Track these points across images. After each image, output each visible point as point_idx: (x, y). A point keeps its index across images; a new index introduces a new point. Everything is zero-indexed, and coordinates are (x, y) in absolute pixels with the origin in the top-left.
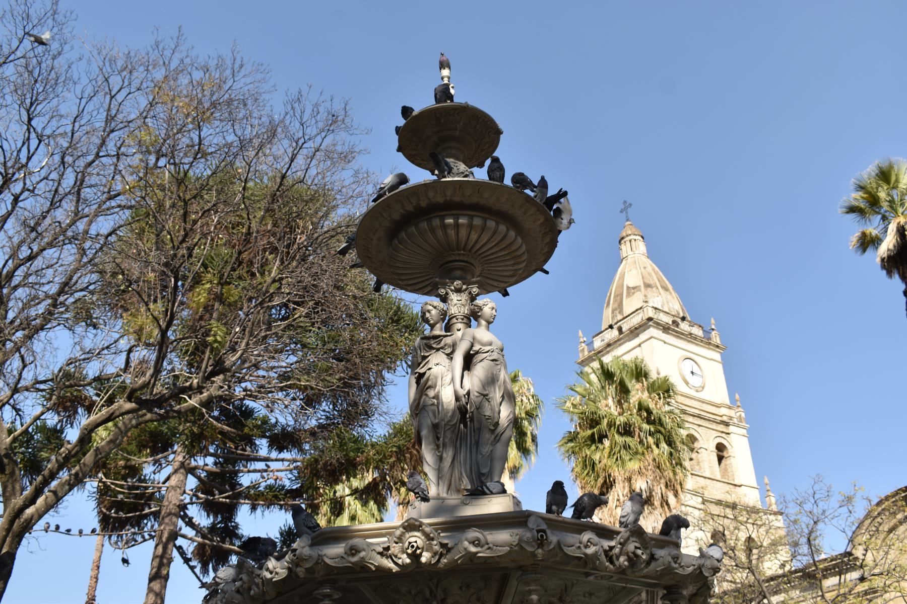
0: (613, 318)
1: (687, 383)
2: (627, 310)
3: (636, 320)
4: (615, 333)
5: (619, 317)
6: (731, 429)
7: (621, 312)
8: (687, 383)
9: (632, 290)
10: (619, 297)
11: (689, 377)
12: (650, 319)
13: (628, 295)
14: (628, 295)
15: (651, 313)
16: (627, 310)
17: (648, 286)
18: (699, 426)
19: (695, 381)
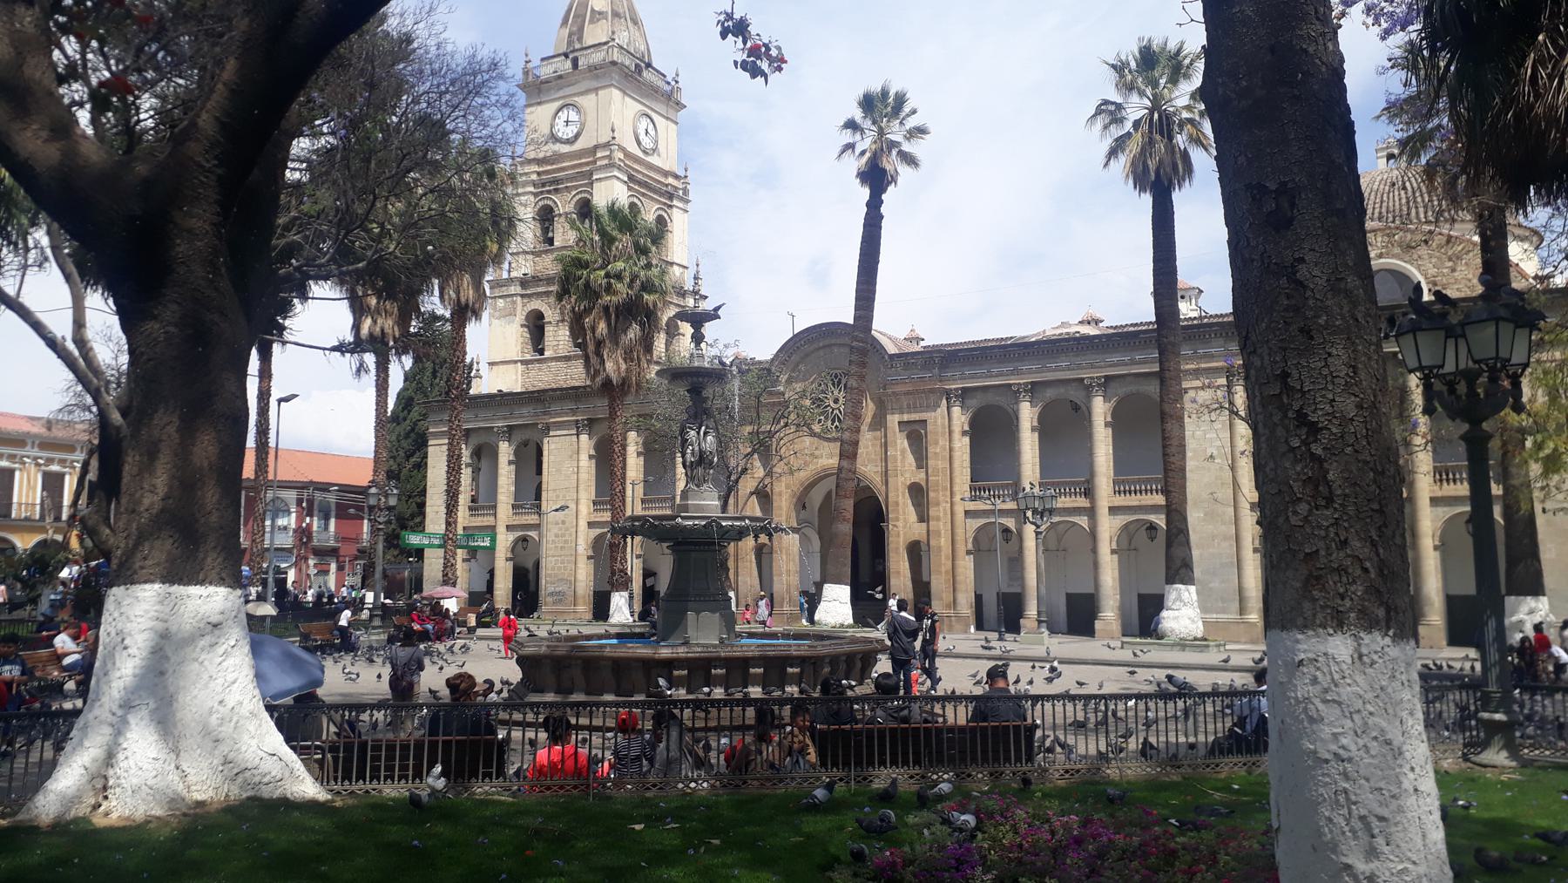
0: (570, 43)
1: (639, 143)
2: (589, 40)
3: (597, 57)
4: (568, 64)
5: (577, 46)
6: (675, 202)
7: (580, 39)
8: (639, 143)
9: (598, 16)
10: (580, 17)
11: (642, 136)
12: (614, 63)
13: (591, 22)
14: (591, 22)
15: (616, 55)
16: (589, 40)
17: (616, 14)
18: (644, 195)
19: (647, 142)
